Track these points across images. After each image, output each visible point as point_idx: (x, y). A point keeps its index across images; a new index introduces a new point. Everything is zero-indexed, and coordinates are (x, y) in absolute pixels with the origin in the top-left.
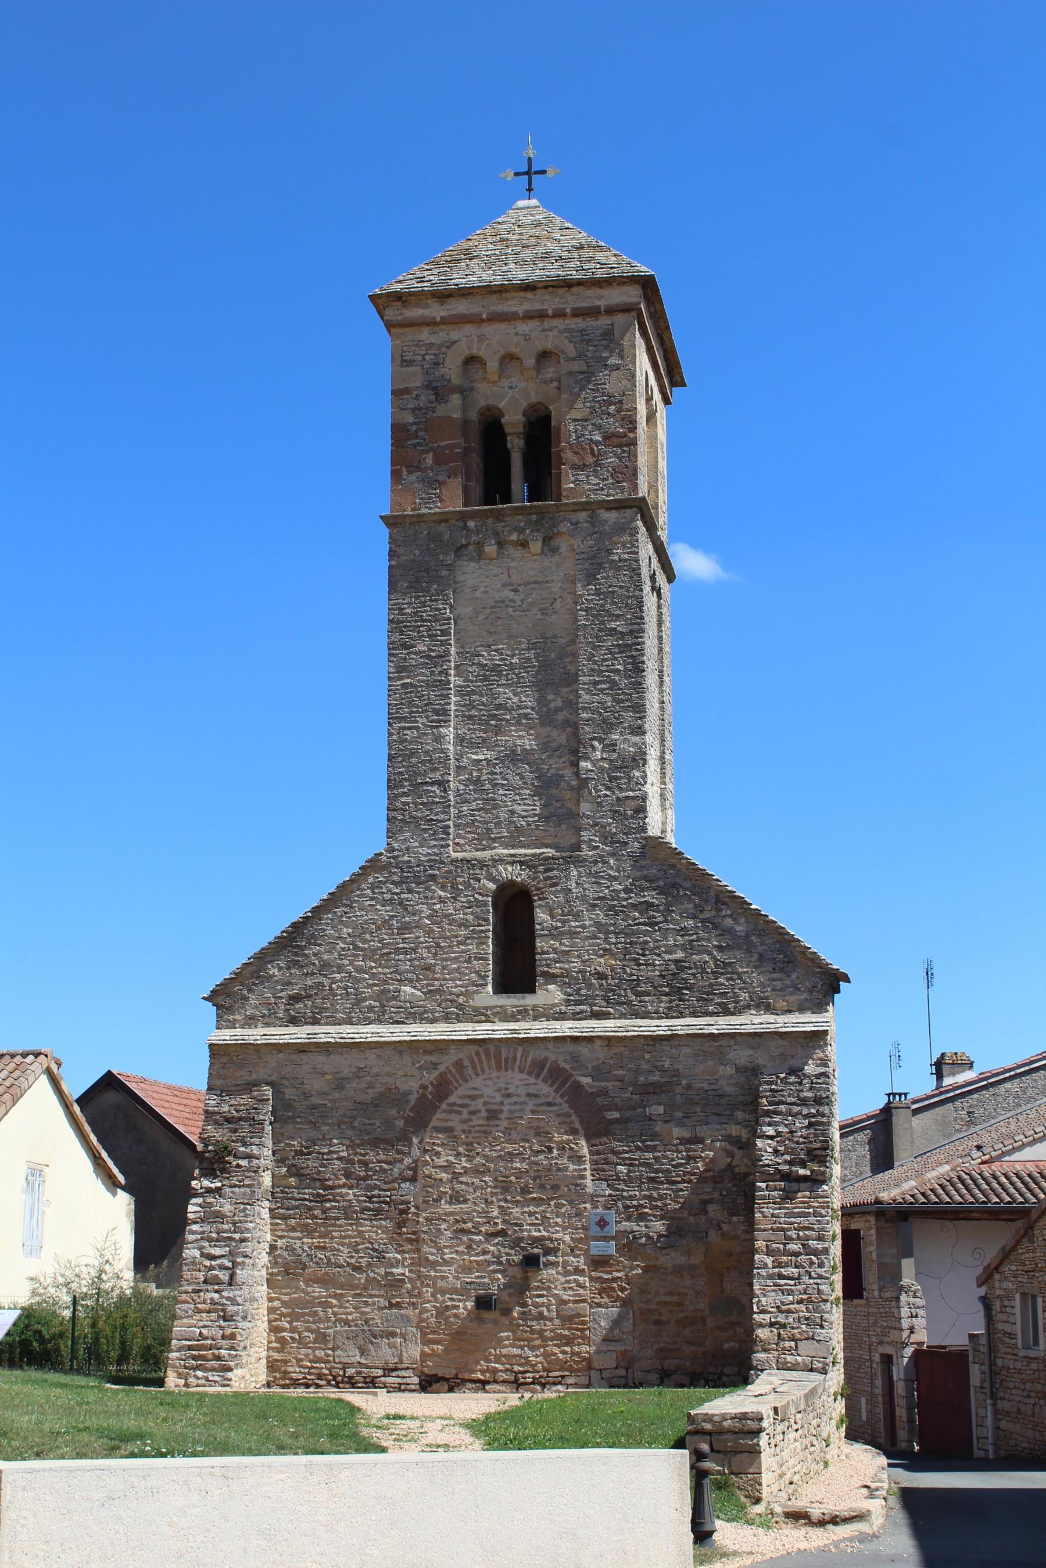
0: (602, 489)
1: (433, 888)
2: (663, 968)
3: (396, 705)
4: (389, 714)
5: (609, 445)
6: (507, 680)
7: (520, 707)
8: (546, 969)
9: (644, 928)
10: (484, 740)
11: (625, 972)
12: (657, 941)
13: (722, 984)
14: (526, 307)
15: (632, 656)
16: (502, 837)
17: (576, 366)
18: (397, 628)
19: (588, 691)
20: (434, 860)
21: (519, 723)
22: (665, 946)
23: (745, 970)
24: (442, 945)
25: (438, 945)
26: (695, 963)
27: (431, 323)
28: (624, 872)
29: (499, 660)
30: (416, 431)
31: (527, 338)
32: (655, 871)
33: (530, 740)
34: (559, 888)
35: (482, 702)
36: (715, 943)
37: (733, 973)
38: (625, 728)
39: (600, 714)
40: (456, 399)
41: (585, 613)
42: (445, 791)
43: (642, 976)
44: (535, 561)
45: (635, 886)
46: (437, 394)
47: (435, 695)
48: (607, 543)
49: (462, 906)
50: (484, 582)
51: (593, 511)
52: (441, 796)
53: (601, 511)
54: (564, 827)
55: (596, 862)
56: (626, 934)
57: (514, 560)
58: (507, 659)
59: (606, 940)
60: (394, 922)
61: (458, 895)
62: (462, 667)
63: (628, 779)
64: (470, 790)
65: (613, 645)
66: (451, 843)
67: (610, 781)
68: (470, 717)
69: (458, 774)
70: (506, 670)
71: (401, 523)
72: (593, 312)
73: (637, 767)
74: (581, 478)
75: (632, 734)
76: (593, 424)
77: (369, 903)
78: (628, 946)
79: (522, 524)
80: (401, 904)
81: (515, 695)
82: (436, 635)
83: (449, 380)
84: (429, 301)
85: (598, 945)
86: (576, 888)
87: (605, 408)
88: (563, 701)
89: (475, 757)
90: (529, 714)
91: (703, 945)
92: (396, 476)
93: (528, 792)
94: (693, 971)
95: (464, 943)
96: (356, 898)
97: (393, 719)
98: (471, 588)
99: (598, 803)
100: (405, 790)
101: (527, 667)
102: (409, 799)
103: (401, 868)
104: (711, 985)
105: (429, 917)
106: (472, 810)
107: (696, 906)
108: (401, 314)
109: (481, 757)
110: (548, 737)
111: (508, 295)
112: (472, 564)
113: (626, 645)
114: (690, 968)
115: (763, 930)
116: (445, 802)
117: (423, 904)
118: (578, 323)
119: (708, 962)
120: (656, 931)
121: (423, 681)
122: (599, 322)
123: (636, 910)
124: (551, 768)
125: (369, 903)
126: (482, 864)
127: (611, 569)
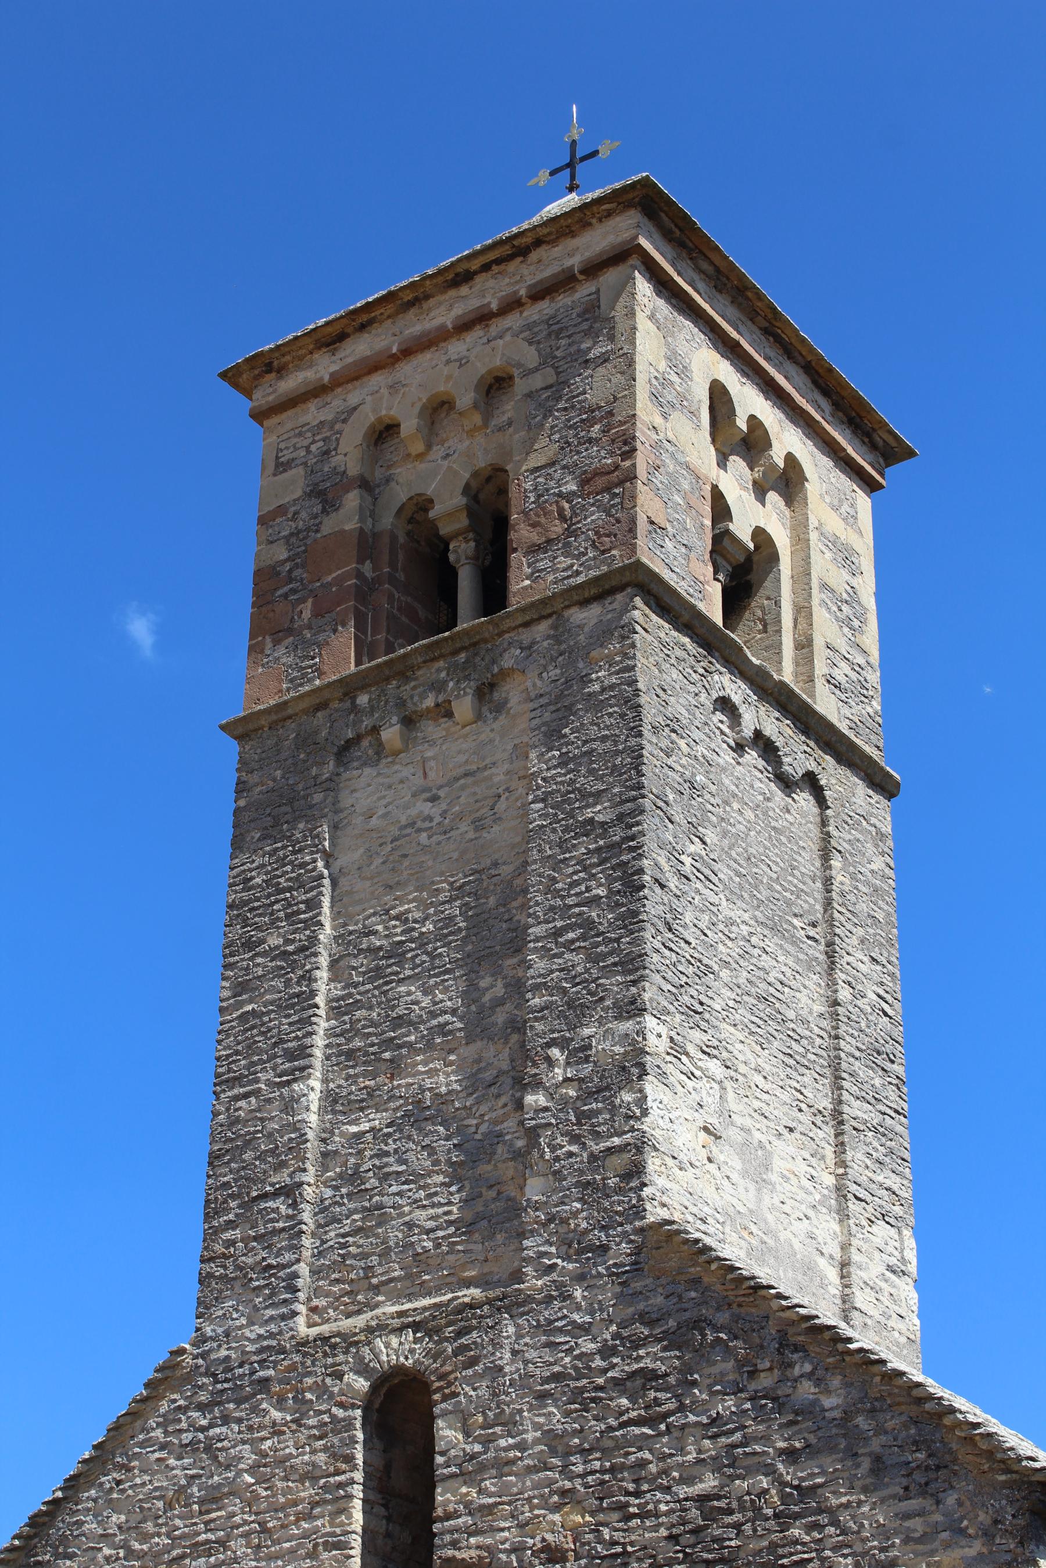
0: (578, 573)
1: (264, 1405)
2: (674, 1518)
3: (228, 1056)
4: (218, 1075)
5: (589, 494)
6: (413, 969)
7: (433, 1015)
8: (450, 1553)
9: (637, 1430)
10: (371, 1092)
11: (600, 1540)
12: (663, 1457)
13: (796, 1542)
14: (459, 310)
15: (624, 864)
16: (391, 1280)
17: (537, 381)
18: (238, 916)
19: (545, 953)
20: (268, 1347)
21: (430, 1045)
22: (680, 1466)
23: (844, 1500)
24: (270, 1525)
25: (264, 1530)
26: (740, 1499)
27: (318, 391)
28: (601, 1310)
29: (403, 933)
30: (290, 571)
31: (462, 362)
32: (659, 1300)
33: (448, 1075)
34: (479, 1368)
35: (371, 1021)
36: (781, 1444)
37: (820, 1511)
38: (606, 1009)
39: (564, 991)
40: (352, 500)
41: (541, 805)
42: (294, 1205)
43: (632, 1544)
44: (466, 736)
45: (622, 1339)
46: (325, 502)
47: (290, 1024)
48: (581, 665)
49: (310, 1437)
50: (384, 797)
51: (558, 614)
52: (289, 1217)
53: (573, 610)
54: (500, 1238)
55: (549, 1300)
56: (603, 1451)
57: (432, 743)
58: (413, 929)
59: (564, 1470)
60: (195, 1489)
61: (304, 1415)
62: (341, 963)
63: (610, 1111)
64: (342, 1197)
65: (589, 851)
66: (302, 1308)
67: (579, 1123)
68: (350, 1054)
69: (325, 1168)
70: (412, 950)
71: (256, 730)
72: (565, 281)
73: (628, 1083)
74: (541, 565)
75: (619, 1018)
76: (564, 467)
77: (157, 1455)
78: (607, 1477)
79: (443, 674)
80: (208, 1449)
81: (425, 993)
82: (299, 912)
83: (344, 472)
84: (316, 356)
85: (552, 1482)
86: (513, 1362)
87: (583, 434)
88: (506, 986)
89: (354, 1129)
90: (447, 1023)
91: (755, 1453)
92: (255, 649)
93: (440, 1178)
94: (737, 1517)
95: (309, 1517)
96: (137, 1450)
97: (222, 1082)
98: (363, 814)
99: (555, 1173)
100: (231, 1216)
101: (446, 936)
102: (237, 1233)
103: (214, 1375)
104: (773, 1546)
105: (252, 1470)
106: (343, 1236)
107: (740, 1364)
108: (274, 391)
109: (365, 1126)
110: (479, 1061)
111: (432, 302)
112: (367, 771)
113: (611, 846)
114: (730, 1512)
115: (882, 1398)
116: (292, 1227)
117: (244, 1442)
118: (545, 308)
119: (766, 1491)
120: (660, 1434)
121: (272, 1003)
122: (577, 296)
123: (623, 1393)
124: (483, 1122)
125: (157, 1455)
126: (349, 1341)
127: (587, 711)
